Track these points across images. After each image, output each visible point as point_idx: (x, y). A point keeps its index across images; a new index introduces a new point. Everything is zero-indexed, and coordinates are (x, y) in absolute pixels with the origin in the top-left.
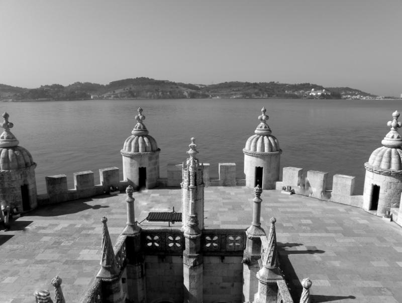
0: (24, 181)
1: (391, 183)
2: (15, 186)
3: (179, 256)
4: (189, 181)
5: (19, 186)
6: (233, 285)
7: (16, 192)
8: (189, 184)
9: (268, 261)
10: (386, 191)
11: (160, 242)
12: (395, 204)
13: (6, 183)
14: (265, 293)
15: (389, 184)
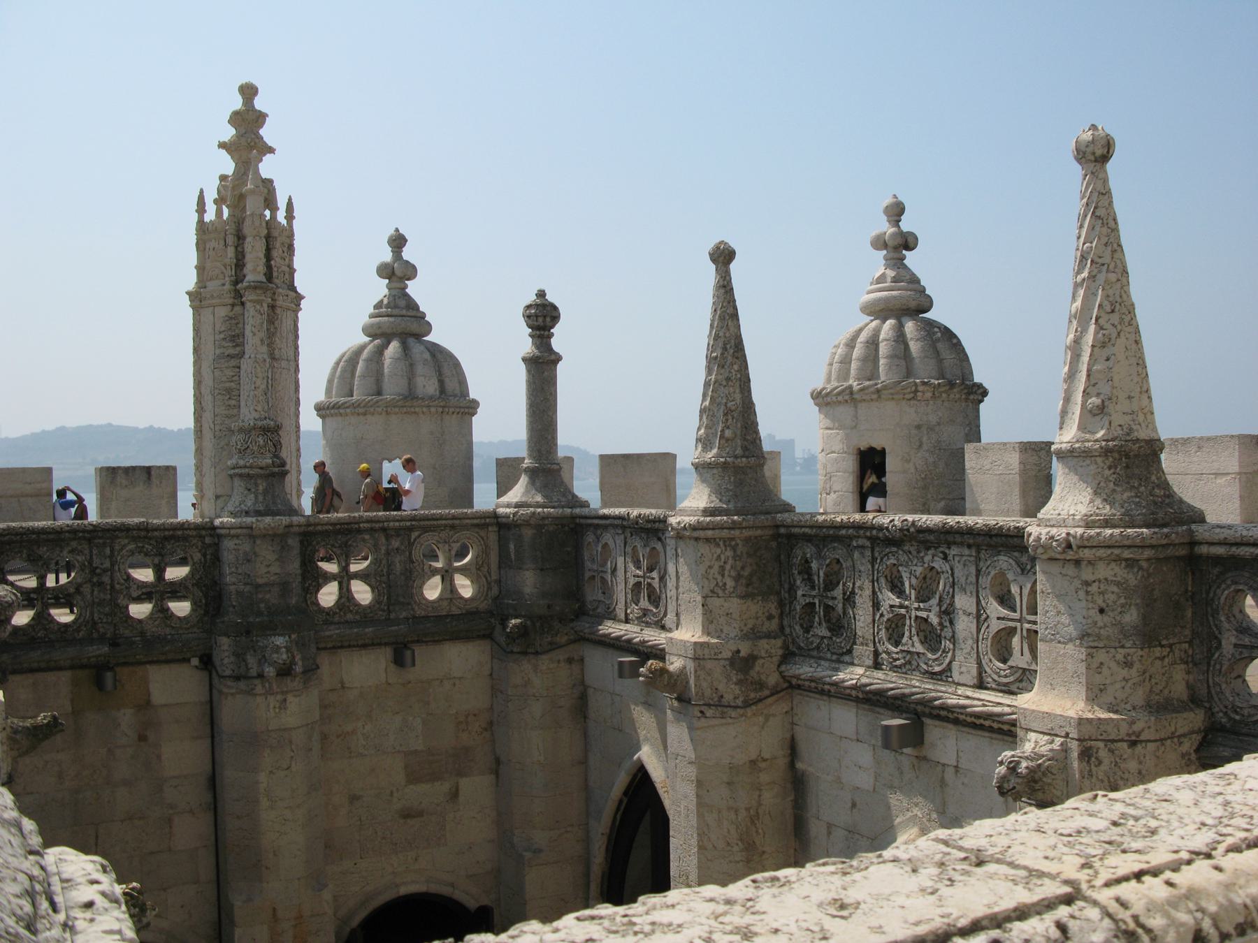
1: (918, 427)
4: (240, 264)
6: (454, 795)
8: (238, 280)
9: (728, 433)
10: (908, 461)
12: (942, 504)
14: (730, 583)
15: (914, 432)
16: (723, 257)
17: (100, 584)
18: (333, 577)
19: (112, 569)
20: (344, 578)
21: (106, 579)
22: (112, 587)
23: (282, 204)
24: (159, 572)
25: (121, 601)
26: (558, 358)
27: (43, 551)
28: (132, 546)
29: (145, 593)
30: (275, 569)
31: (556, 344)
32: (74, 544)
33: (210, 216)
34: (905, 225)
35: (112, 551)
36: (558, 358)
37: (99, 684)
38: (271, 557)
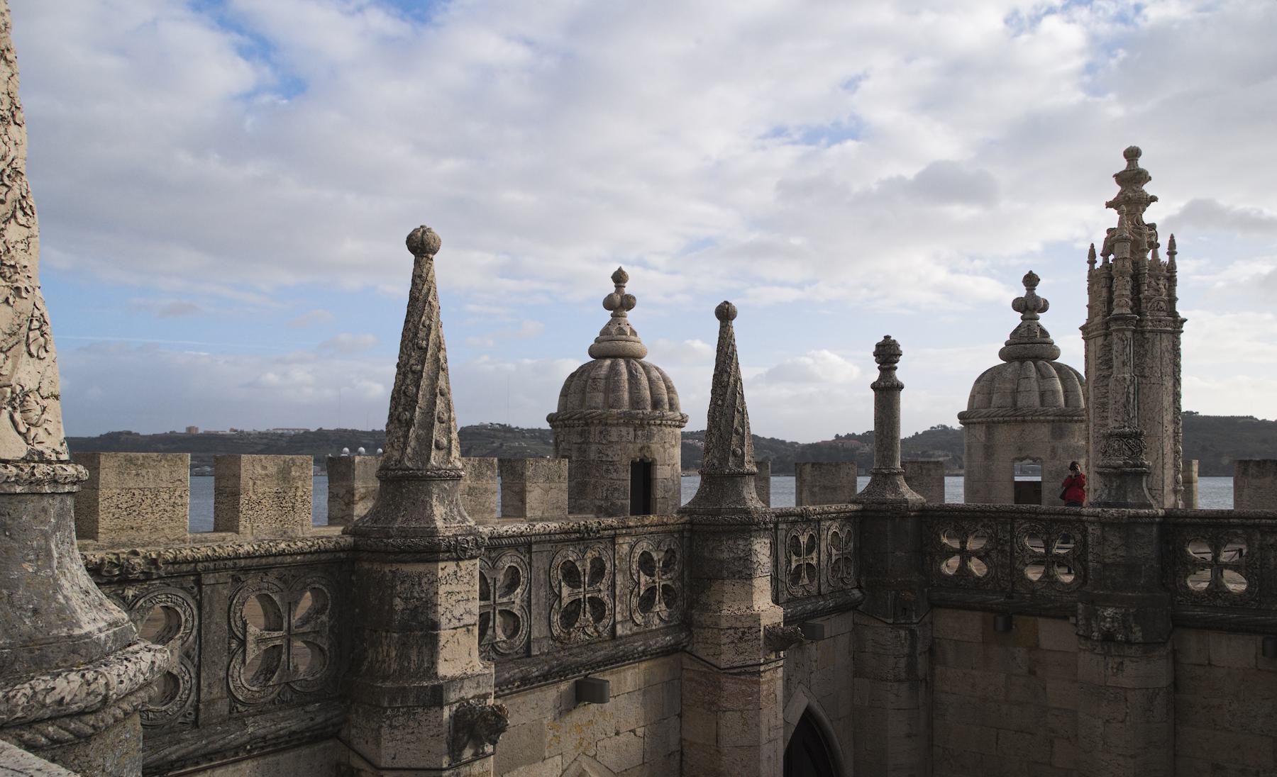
0: (641, 449)
2: (616, 459)
3: (1066, 618)
5: (626, 461)
7: (614, 476)
11: (993, 554)
13: (594, 447)
16: (725, 314)
17: (1003, 551)
18: (1203, 565)
19: (1012, 542)
20: (1218, 567)
21: (1007, 548)
22: (1012, 554)
23: (1163, 241)
24: (1048, 546)
25: (1018, 565)
26: (900, 387)
27: (965, 524)
28: (1027, 525)
29: (1038, 561)
30: (1121, 552)
31: (900, 374)
32: (986, 521)
33: (1100, 261)
34: (628, 289)
35: (1012, 528)
36: (900, 387)
37: (1008, 627)
38: (1117, 542)
